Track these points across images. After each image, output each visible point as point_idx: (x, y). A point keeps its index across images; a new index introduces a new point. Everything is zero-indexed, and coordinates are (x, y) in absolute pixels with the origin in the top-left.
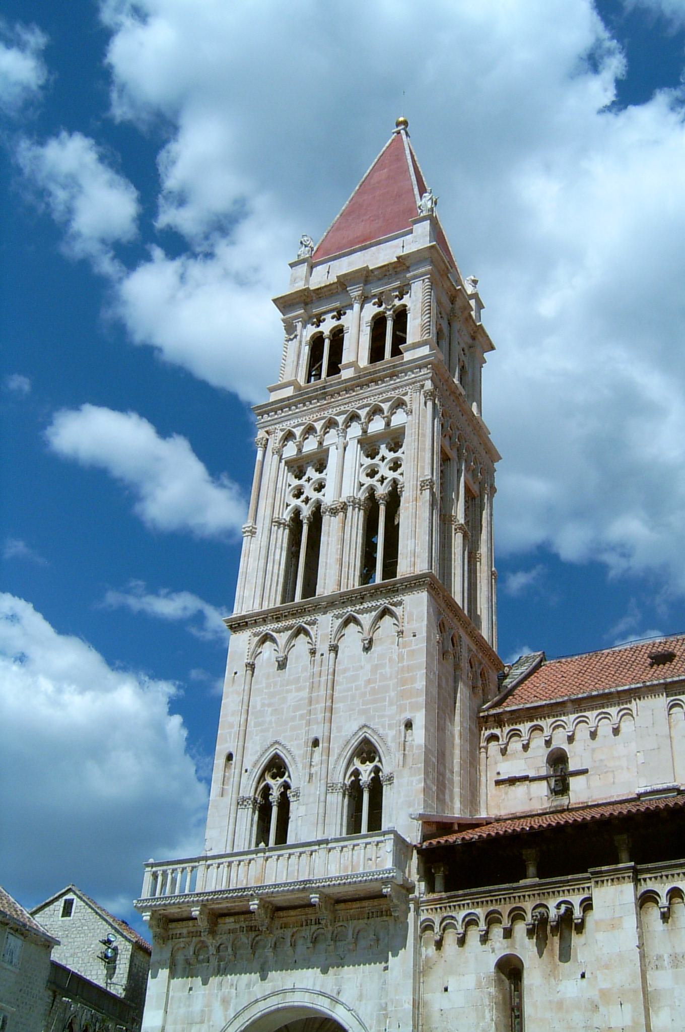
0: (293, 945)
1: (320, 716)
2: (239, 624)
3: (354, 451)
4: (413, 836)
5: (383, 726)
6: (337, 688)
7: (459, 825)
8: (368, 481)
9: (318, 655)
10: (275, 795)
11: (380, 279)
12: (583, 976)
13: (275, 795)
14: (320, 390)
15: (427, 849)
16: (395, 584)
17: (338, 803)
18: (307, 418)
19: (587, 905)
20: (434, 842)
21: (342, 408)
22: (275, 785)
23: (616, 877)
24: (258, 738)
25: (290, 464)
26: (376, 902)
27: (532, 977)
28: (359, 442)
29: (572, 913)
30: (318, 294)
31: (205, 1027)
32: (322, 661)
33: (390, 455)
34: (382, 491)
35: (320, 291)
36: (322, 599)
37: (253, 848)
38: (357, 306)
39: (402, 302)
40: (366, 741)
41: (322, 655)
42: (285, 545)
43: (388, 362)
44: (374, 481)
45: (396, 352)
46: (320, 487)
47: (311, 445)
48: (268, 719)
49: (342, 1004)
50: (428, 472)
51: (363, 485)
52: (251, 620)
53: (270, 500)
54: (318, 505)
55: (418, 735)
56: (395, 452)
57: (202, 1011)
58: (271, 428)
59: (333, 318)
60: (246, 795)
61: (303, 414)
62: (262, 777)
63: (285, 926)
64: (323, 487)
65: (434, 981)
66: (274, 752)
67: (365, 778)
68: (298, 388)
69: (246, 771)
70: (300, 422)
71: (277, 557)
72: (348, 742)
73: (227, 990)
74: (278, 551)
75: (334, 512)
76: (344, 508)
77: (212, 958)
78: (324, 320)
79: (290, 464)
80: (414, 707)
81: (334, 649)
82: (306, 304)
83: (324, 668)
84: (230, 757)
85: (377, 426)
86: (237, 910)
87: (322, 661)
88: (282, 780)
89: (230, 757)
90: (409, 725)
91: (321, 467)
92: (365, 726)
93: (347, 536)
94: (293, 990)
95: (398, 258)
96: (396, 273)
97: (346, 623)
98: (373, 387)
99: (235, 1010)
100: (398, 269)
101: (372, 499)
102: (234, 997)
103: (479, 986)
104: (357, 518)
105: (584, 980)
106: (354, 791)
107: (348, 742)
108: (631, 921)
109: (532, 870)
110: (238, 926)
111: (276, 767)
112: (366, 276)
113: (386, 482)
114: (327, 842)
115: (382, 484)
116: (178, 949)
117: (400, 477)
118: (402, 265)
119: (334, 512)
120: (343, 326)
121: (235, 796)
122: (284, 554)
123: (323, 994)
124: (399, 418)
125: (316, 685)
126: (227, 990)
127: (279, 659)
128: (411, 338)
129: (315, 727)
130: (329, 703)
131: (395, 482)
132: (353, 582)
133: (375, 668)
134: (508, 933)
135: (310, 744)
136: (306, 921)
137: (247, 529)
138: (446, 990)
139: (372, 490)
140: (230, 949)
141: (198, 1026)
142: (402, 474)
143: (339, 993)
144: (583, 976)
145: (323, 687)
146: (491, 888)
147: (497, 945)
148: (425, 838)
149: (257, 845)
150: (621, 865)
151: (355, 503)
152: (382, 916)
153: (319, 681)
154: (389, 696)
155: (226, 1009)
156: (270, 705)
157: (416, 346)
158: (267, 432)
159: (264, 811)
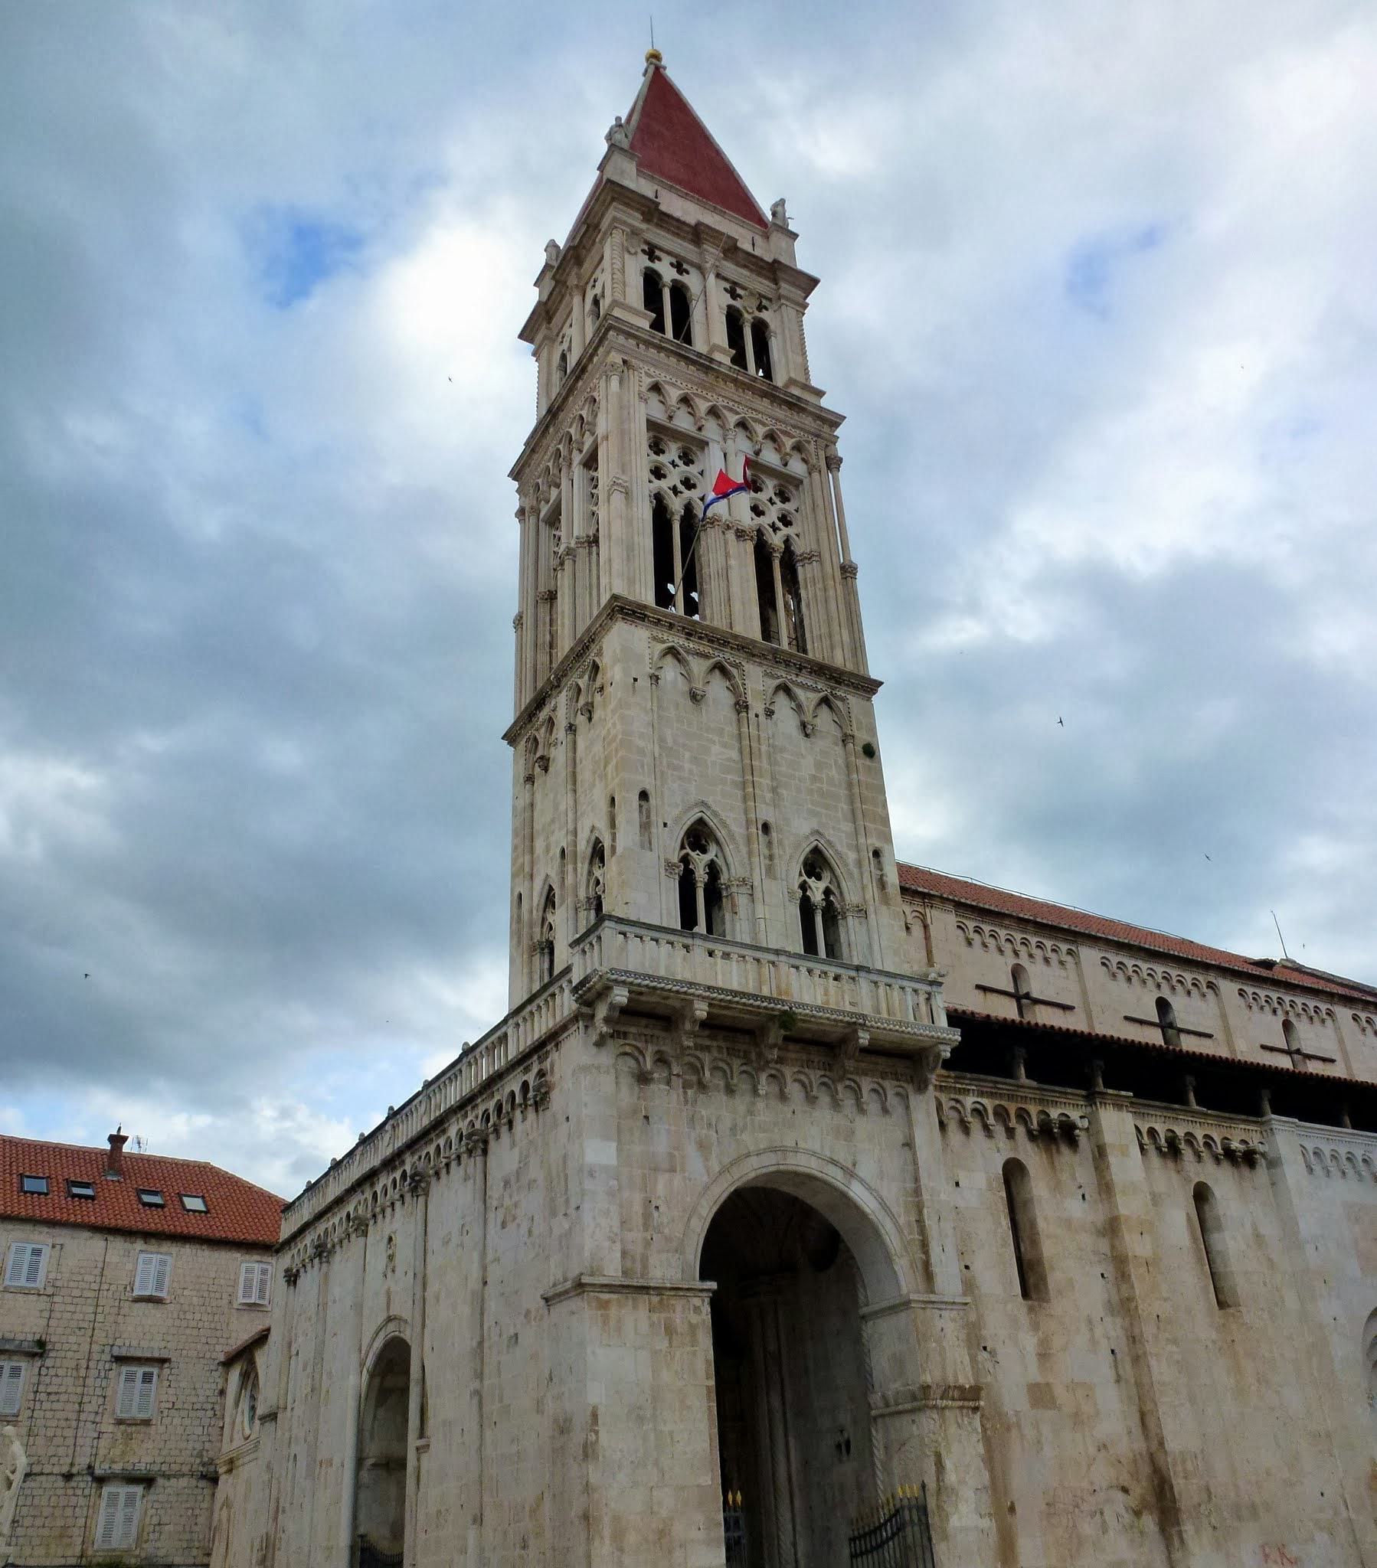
2: (634, 612)
9: (751, 715)
10: (701, 876)
11: (737, 264)
13: (701, 876)
14: (705, 360)
18: (684, 384)
21: (731, 404)
22: (700, 862)
24: (676, 785)
27: (1038, 1186)
30: (661, 220)
31: (677, 1180)
32: (758, 725)
33: (779, 505)
35: (666, 219)
40: (816, 851)
47: (683, 422)
49: (862, 1181)
52: (653, 618)
57: (671, 1156)
58: (634, 361)
59: (672, 264)
66: (700, 814)
67: (817, 896)
69: (665, 825)
70: (679, 383)
73: (704, 1132)
77: (673, 1077)
79: (652, 425)
81: (770, 713)
85: (770, 457)
87: (758, 725)
89: (644, 796)
91: (687, 458)
94: (796, 1150)
95: (775, 261)
96: (759, 274)
98: (766, 402)
99: (720, 1163)
100: (764, 272)
102: (716, 1144)
103: (990, 1188)
105: (1086, 1201)
106: (806, 908)
110: (715, 1044)
111: (698, 836)
112: (731, 250)
123: (834, 1162)
126: (704, 1131)
127: (698, 692)
129: (763, 806)
131: (787, 541)
135: (760, 827)
136: (808, 1061)
137: (620, 481)
138: (957, 1184)
141: (667, 1175)
142: (798, 535)
143: (854, 1165)
146: (998, 1079)
147: (1001, 1145)
152: (898, 1080)
153: (760, 749)
154: (842, 808)
158: (625, 362)
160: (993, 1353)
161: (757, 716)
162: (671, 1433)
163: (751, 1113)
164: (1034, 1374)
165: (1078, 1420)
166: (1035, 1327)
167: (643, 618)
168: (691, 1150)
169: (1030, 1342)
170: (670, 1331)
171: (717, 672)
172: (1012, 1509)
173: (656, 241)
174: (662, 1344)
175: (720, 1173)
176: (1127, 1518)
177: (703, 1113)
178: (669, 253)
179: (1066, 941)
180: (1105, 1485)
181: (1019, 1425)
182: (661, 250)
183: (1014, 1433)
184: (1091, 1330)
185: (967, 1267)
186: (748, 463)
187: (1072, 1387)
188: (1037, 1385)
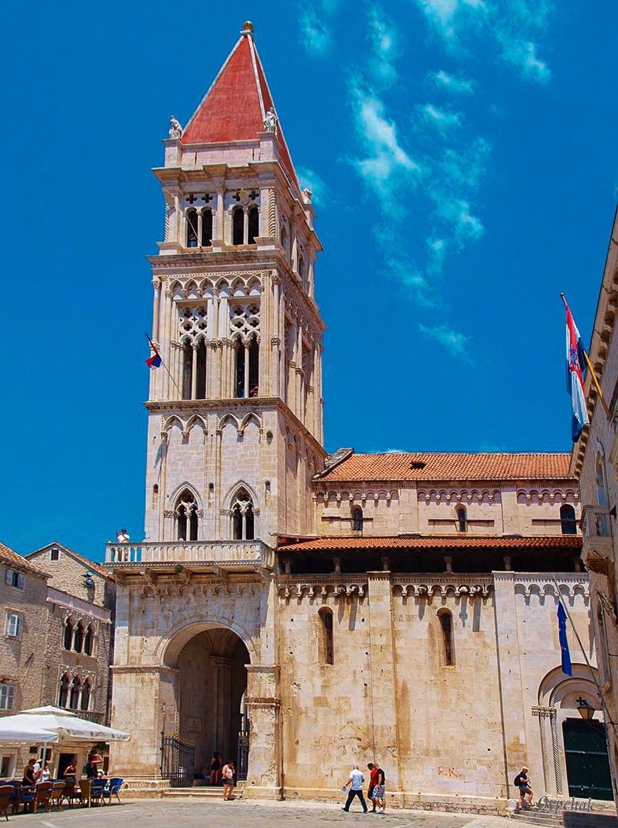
0: (205, 593)
1: (213, 472)
3: (225, 309)
4: (272, 543)
5: (253, 482)
6: (223, 456)
7: (299, 539)
9: (209, 435)
12: (363, 620)
15: (279, 551)
16: (256, 401)
17: (228, 523)
19: (366, 588)
20: (284, 548)
23: (381, 577)
26: (252, 575)
28: (228, 300)
29: (359, 591)
34: (246, 338)
36: (210, 402)
37: (176, 540)
38: (220, 198)
41: (212, 435)
42: (182, 361)
43: (246, 247)
45: (251, 241)
46: (203, 326)
48: (179, 468)
50: (276, 333)
51: (233, 331)
53: (167, 329)
54: (202, 339)
55: (274, 490)
56: (254, 314)
59: (203, 199)
60: (169, 510)
61: (187, 272)
62: (178, 501)
63: (200, 582)
64: (206, 326)
65: (286, 615)
67: (243, 509)
68: (182, 250)
71: (177, 368)
72: (232, 488)
74: (177, 365)
75: (214, 346)
78: (196, 199)
80: (272, 474)
81: (219, 433)
82: (180, 181)
83: (214, 443)
84: (156, 487)
86: (169, 572)
88: (191, 504)
89: (156, 487)
90: (268, 484)
92: (241, 481)
93: (224, 364)
97: (226, 419)
99: (173, 623)
104: (230, 354)
106: (237, 516)
107: (232, 488)
108: (387, 598)
109: (337, 568)
110: (171, 580)
113: (248, 333)
114: (222, 542)
116: (133, 591)
117: (258, 332)
118: (251, 171)
119: (214, 346)
121: (162, 511)
122: (182, 366)
124: (254, 293)
125: (209, 452)
128: (261, 235)
130: (218, 464)
132: (230, 395)
133: (246, 448)
134: (325, 597)
135: (208, 486)
138: (292, 620)
140: (166, 592)
141: (151, 629)
142: (259, 330)
144: (363, 620)
145: (214, 454)
148: (279, 545)
149: (179, 538)
150: (383, 572)
151: (228, 343)
155: (167, 622)
156: (180, 460)
157: (265, 242)
158: (160, 278)
159: (182, 520)
160: (298, 685)
161: (212, 435)
162: (140, 714)
163: (188, 603)
164: (319, 693)
165: (339, 711)
166: (323, 675)
167: (159, 408)
168: (161, 619)
169: (319, 681)
170: (143, 681)
171: (198, 420)
172: (297, 742)
173: (192, 190)
174: (140, 685)
175: (173, 627)
176: (358, 750)
177: (168, 606)
178: (200, 193)
179: (493, 486)
180: (348, 736)
181: (306, 713)
182: (196, 193)
183: (304, 715)
184: (355, 676)
185: (291, 653)
187: (340, 698)
188: (320, 697)
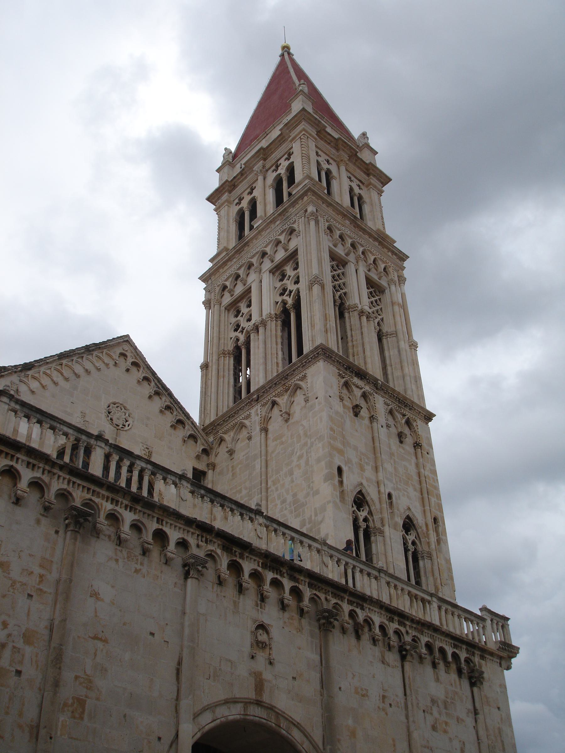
8: (279, 299)
25: (228, 308)
28: (270, 272)
34: (290, 301)
39: (291, 160)
44: (285, 297)
47: (239, 289)
59: (248, 194)
76: (263, 323)
78: (243, 198)
81: (265, 430)
85: (280, 255)
101: (285, 312)
104: (274, 327)
113: (292, 294)
115: (290, 297)
120: (255, 196)
139: (284, 303)
186: (272, 271)
